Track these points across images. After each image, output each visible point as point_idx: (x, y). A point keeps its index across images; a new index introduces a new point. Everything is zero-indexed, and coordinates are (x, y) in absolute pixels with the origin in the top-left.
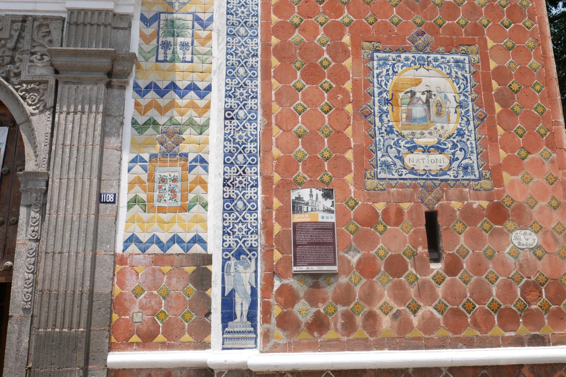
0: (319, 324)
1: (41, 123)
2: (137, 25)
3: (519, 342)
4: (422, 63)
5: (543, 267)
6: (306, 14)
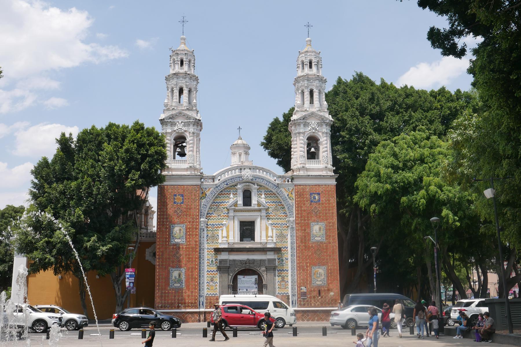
0: (304, 305)
1: (265, 276)
2: (277, 260)
3: (330, 307)
4: (319, 268)
5: (334, 297)
6: (303, 260)
